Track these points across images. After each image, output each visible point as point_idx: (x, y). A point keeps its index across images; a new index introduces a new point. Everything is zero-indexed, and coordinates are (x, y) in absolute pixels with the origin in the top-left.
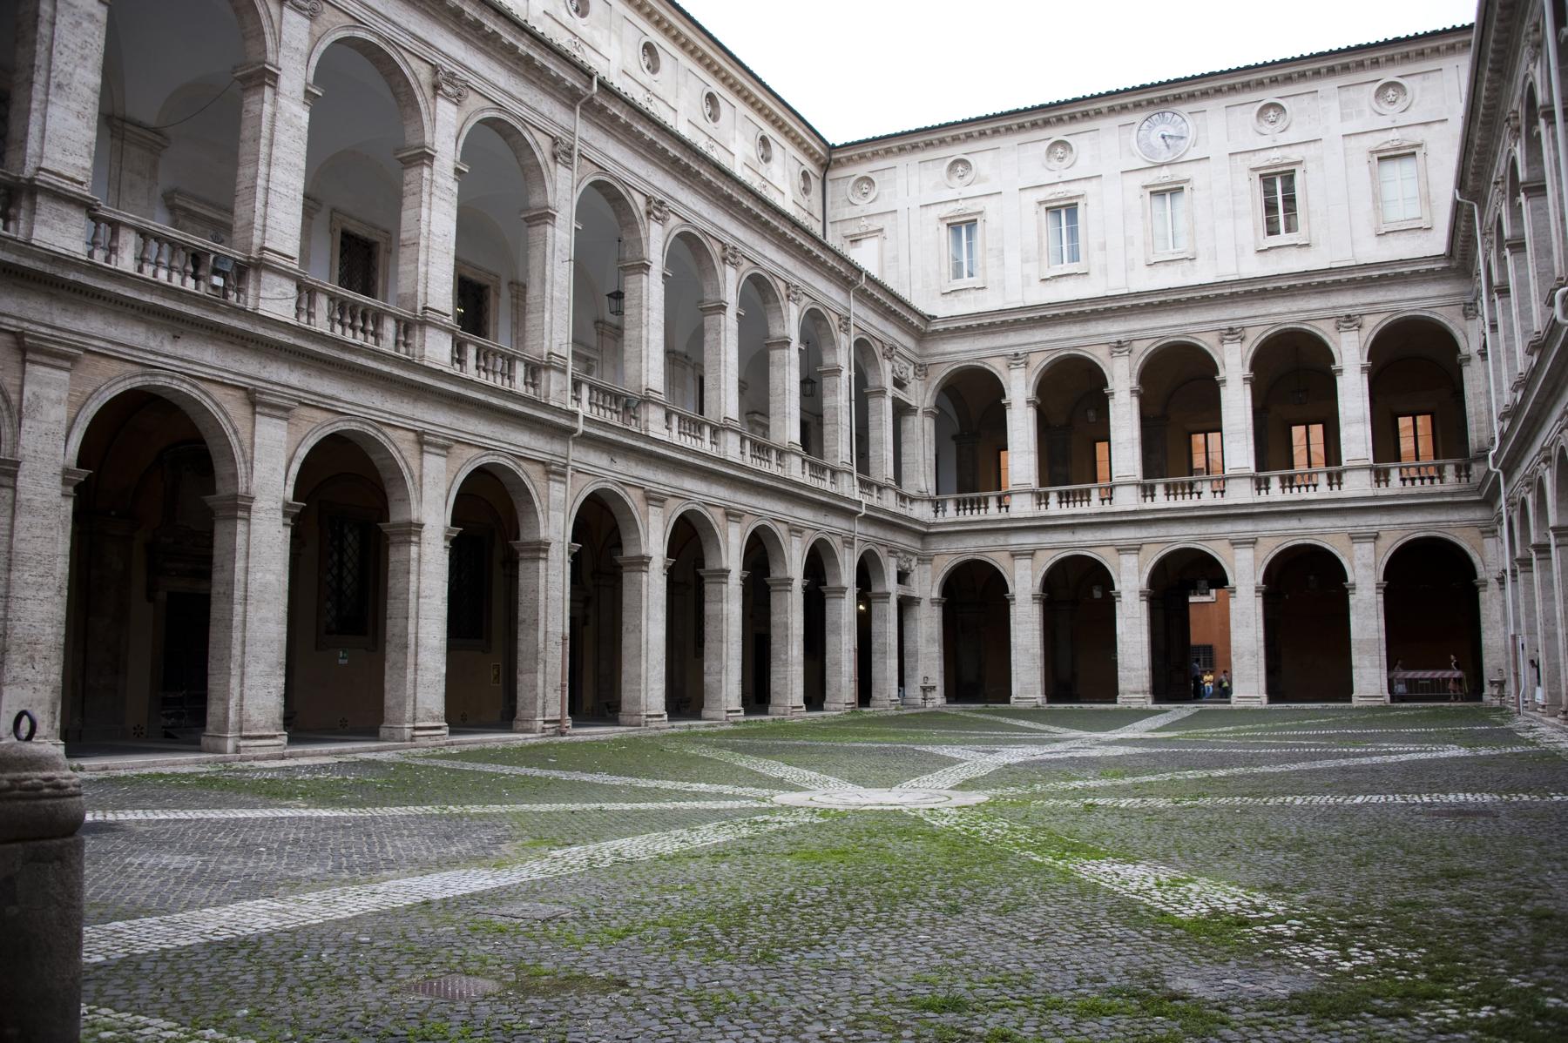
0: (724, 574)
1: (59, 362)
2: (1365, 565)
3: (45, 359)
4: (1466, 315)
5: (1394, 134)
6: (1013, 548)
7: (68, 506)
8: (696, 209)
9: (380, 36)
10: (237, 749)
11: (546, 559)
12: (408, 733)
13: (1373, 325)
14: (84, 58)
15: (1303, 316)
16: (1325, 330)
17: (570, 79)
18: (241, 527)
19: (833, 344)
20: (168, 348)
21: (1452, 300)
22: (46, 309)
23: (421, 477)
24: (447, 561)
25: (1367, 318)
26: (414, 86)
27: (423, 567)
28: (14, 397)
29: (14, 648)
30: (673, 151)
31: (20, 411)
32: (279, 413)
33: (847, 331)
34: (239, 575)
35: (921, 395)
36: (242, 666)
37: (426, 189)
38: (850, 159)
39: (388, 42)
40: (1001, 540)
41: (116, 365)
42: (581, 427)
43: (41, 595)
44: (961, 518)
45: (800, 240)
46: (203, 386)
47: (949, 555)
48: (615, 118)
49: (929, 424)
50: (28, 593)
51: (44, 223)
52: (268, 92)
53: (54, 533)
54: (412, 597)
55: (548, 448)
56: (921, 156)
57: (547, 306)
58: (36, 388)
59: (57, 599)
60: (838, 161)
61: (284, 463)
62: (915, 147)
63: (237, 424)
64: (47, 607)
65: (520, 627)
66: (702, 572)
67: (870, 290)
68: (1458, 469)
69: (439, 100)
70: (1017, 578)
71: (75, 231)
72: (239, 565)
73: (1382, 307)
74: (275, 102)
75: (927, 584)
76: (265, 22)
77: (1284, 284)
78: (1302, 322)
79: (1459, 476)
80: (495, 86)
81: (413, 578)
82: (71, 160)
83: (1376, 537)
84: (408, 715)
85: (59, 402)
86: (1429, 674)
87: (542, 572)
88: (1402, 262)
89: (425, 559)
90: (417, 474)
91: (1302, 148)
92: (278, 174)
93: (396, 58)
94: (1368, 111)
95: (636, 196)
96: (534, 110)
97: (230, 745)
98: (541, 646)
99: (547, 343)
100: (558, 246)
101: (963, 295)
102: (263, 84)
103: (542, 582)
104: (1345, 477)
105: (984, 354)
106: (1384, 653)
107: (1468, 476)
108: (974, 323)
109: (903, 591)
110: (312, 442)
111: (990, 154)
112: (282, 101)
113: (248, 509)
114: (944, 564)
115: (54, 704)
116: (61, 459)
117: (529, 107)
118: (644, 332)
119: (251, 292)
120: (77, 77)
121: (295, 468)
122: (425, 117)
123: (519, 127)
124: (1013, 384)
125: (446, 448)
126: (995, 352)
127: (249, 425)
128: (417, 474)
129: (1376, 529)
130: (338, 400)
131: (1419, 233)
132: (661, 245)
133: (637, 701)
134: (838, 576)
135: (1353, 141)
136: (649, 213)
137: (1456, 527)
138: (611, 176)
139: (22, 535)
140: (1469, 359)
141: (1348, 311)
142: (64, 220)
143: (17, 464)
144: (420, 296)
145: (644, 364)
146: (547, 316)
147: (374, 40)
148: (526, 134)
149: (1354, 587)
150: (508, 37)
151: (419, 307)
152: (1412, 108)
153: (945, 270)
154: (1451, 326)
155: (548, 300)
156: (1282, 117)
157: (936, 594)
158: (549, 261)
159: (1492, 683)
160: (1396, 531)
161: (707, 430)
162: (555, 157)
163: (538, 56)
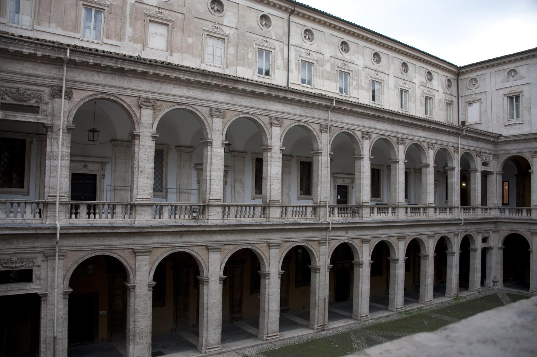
0: (397, 260)
1: (146, 254)
3: (142, 254)
6: (532, 231)
7: (151, 293)
8: (385, 129)
9: (249, 114)
10: (205, 353)
11: (319, 272)
12: (265, 338)
14: (148, 160)
17: (324, 103)
18: (205, 287)
19: (451, 159)
20: (179, 240)
22: (141, 239)
23: (269, 257)
24: (280, 282)
26: (263, 126)
27: (271, 286)
28: (133, 266)
30: (371, 113)
32: (217, 250)
33: (458, 152)
34: (205, 301)
35: (495, 167)
36: (207, 328)
37: (269, 160)
38: (467, 71)
40: (527, 226)
41: (163, 249)
44: (511, 216)
45: (432, 126)
46: (191, 248)
47: (506, 230)
48: (345, 109)
49: (499, 178)
50: (140, 320)
51: (139, 214)
52: (209, 148)
54: (267, 296)
55: (320, 235)
56: (496, 69)
57: (320, 185)
58: (139, 263)
59: (149, 319)
60: (462, 72)
61: (219, 265)
62: (493, 65)
63: (203, 257)
64: (146, 322)
65: (311, 294)
66: (389, 258)
67: (468, 134)
69: (273, 128)
70: (534, 243)
71: (149, 213)
72: (205, 298)
74: (212, 150)
75: (496, 242)
76: (207, 125)
80: (295, 115)
81: (267, 290)
82: (146, 192)
84: (265, 332)
87: (317, 277)
89: (271, 283)
90: (267, 257)
92: (214, 174)
93: (256, 118)
96: (312, 117)
97: (203, 351)
98: (317, 301)
99: (319, 198)
100: (323, 162)
101: (514, 127)
102: (207, 146)
103: (317, 280)
105: (522, 151)
108: (517, 139)
109: (486, 245)
110: (229, 256)
111: (526, 67)
112: (214, 149)
113: (208, 282)
114: (504, 234)
115: (149, 348)
116: (148, 281)
117: (309, 117)
118: (362, 182)
119: (207, 214)
120: (146, 167)
121: (223, 265)
122: (268, 135)
123: (306, 125)
124: (534, 163)
125: (279, 246)
126: (526, 150)
127: (207, 256)
128: (267, 257)
132: (368, 148)
133: (357, 311)
134: (452, 247)
136: (363, 137)
142: (144, 211)
143: (135, 286)
144: (268, 197)
145: (361, 193)
146: (319, 189)
147: (247, 116)
148: (309, 127)
150: (297, 98)
151: (268, 201)
153: (506, 116)
155: (319, 183)
157: (500, 245)
158: (320, 169)
161: (390, 209)
162: (321, 131)
163: (310, 100)
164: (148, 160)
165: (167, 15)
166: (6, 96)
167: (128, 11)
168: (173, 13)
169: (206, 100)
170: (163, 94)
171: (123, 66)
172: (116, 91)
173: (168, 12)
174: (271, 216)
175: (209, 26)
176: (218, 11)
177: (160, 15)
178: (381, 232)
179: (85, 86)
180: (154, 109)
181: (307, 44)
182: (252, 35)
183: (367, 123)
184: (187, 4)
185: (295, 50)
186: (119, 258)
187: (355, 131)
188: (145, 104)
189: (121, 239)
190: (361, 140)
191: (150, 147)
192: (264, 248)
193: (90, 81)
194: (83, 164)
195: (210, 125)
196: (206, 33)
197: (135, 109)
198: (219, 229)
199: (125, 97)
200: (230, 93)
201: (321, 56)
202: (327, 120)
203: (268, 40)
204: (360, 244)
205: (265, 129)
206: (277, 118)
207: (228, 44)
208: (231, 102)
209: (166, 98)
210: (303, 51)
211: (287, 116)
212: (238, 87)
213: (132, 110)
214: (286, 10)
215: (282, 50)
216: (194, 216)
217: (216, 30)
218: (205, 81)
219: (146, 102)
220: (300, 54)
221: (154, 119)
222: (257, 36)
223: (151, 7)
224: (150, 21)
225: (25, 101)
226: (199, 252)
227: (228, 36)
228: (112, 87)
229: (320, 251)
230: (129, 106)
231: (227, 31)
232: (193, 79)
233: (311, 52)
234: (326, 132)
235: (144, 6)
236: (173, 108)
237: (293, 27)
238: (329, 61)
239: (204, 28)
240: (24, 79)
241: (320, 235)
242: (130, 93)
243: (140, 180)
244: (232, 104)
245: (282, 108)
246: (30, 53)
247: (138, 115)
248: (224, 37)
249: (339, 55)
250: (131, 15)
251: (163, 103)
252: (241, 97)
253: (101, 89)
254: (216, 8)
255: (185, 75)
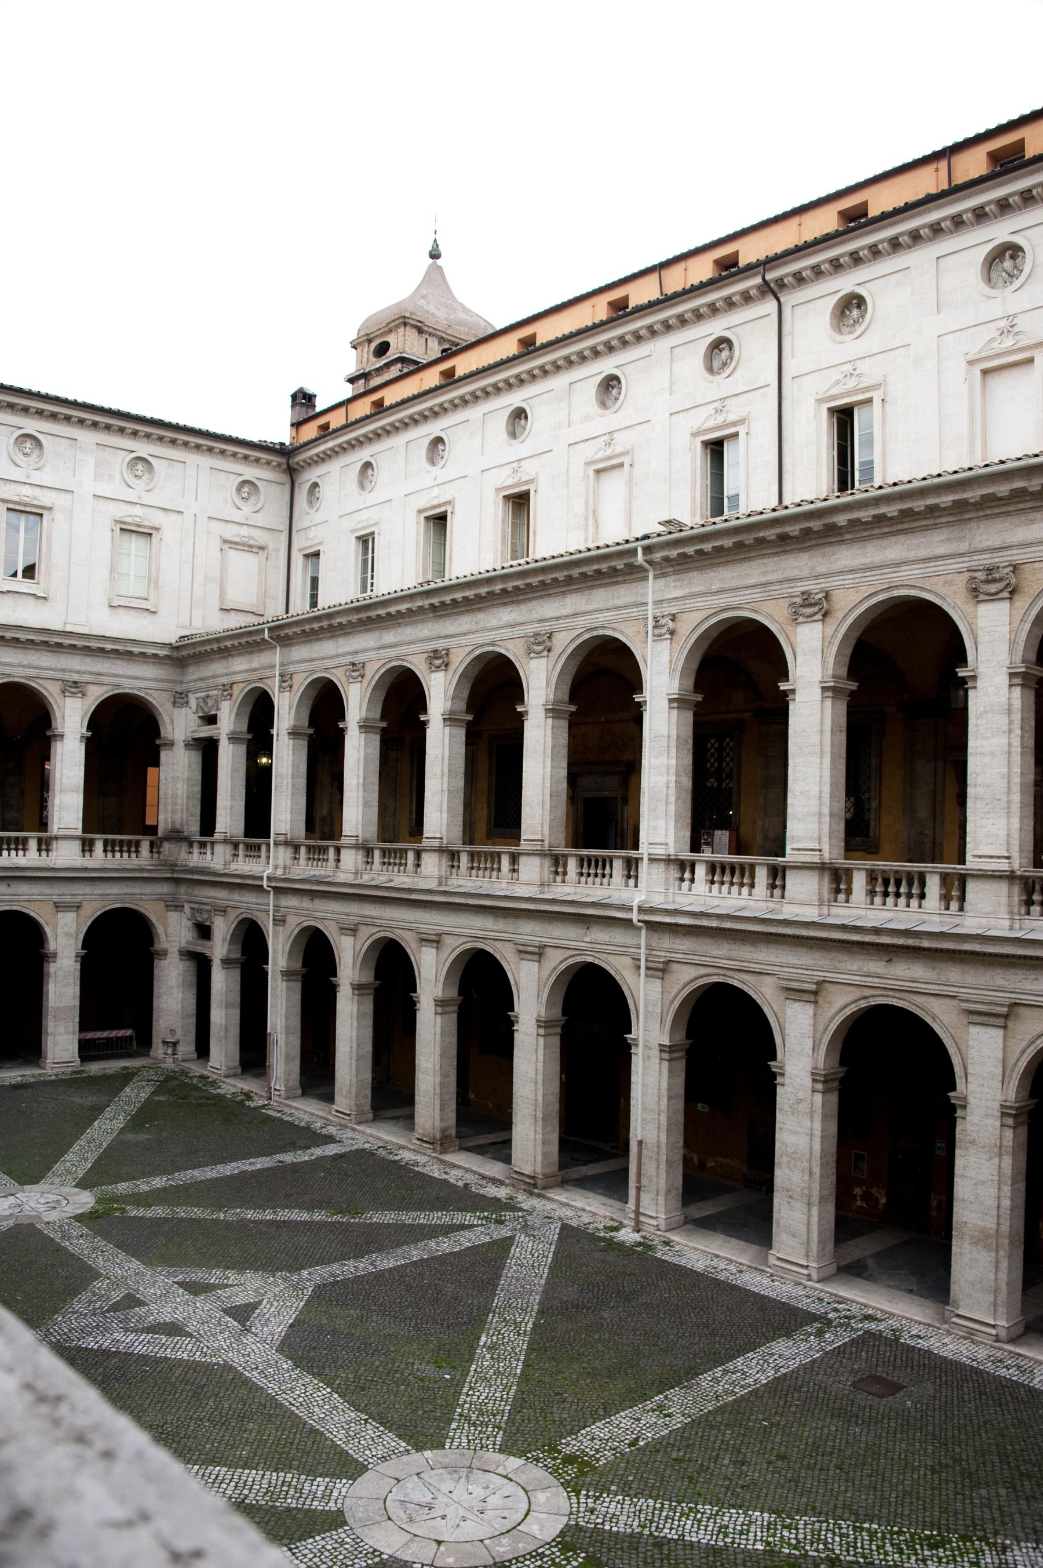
2: (67, 935)
4: (174, 703)
5: (137, 511)
13: (96, 694)
15: (32, 672)
16: (51, 691)
21: (165, 685)
25: (91, 687)
68: (152, 844)
73: (106, 679)
77: (22, 636)
78: (30, 678)
79: (151, 852)
83: (78, 907)
86: (105, 1034)
88: (134, 641)
91: (53, 494)
94: (118, 477)
104: (54, 844)
106: (77, 1020)
107: (159, 852)
129: (79, 899)
131: (146, 614)
135: (101, 505)
137: (146, 900)
140: (171, 744)
141: (75, 677)
149: (55, 955)
152: (156, 490)
154: (160, 710)
156: (36, 452)
159: (165, 1043)
160: (96, 901)
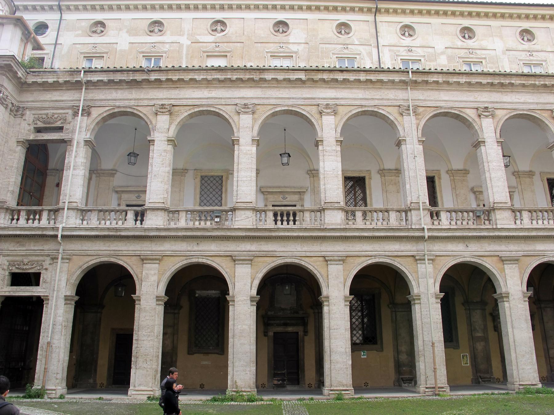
1: (155, 262)
3: (150, 262)
14: (163, 164)
22: (150, 246)
29: (140, 357)
31: (142, 280)
32: (247, 262)
39: (292, 106)
42: (427, 234)
43: (149, 339)
50: (145, 338)
51: (150, 219)
53: (153, 318)
55: (414, 248)
58: (147, 272)
63: (228, 270)
85: (155, 274)
90: (325, 275)
92: (242, 174)
93: (298, 110)
95: (468, 111)
130: (276, 252)
138: (445, 108)
139: (142, 319)
146: (408, 186)
147: (286, 108)
148: (381, 111)
164: (163, 164)
165: (224, 47)
166: (38, 122)
167: (184, 52)
168: (231, 44)
169: (230, 98)
170: (180, 99)
171: (135, 78)
172: (132, 103)
173: (225, 44)
174: (326, 221)
175: (272, 48)
176: (284, 32)
177: (217, 49)
178: (540, 247)
179: (103, 103)
180: (171, 114)
181: (407, 41)
182: (327, 46)
183: (485, 98)
184: (245, 33)
185: (390, 50)
186: (125, 265)
187: (463, 110)
188: (161, 110)
189: (128, 244)
190: (477, 119)
191: (165, 151)
192: (318, 263)
193: (109, 97)
194: (137, 195)
195: (237, 123)
196: (269, 54)
197: (150, 117)
198: (244, 234)
199: (141, 107)
200: (260, 87)
201: (430, 50)
202: (408, 100)
203: (349, 46)
204: (500, 265)
205: (313, 121)
206: (327, 105)
207: (296, 60)
208: (263, 96)
209: (185, 102)
210: (402, 49)
211: (343, 102)
212: (266, 77)
213: (148, 118)
214: (369, 10)
215: (370, 54)
216: (217, 222)
217: (281, 50)
218: (223, 77)
219: (162, 108)
220: (397, 54)
221: (171, 124)
222: (334, 46)
223: (208, 44)
224: (208, 56)
225: (52, 123)
226: (223, 264)
227: (296, 53)
228: (128, 99)
229: (417, 272)
230: (145, 114)
231: (294, 48)
232: (209, 77)
233: (413, 49)
234: (409, 114)
235: (201, 44)
236: (193, 111)
237: (382, 28)
238: (443, 53)
239: (267, 51)
240: (52, 104)
241: (414, 248)
242: (146, 103)
243: (152, 184)
244: (263, 98)
245: (335, 94)
246: (54, 81)
247: (154, 122)
248: (291, 55)
249: (459, 44)
250: (187, 54)
251: (181, 108)
252: (276, 90)
253: (117, 104)
254: (281, 30)
255: (200, 75)
